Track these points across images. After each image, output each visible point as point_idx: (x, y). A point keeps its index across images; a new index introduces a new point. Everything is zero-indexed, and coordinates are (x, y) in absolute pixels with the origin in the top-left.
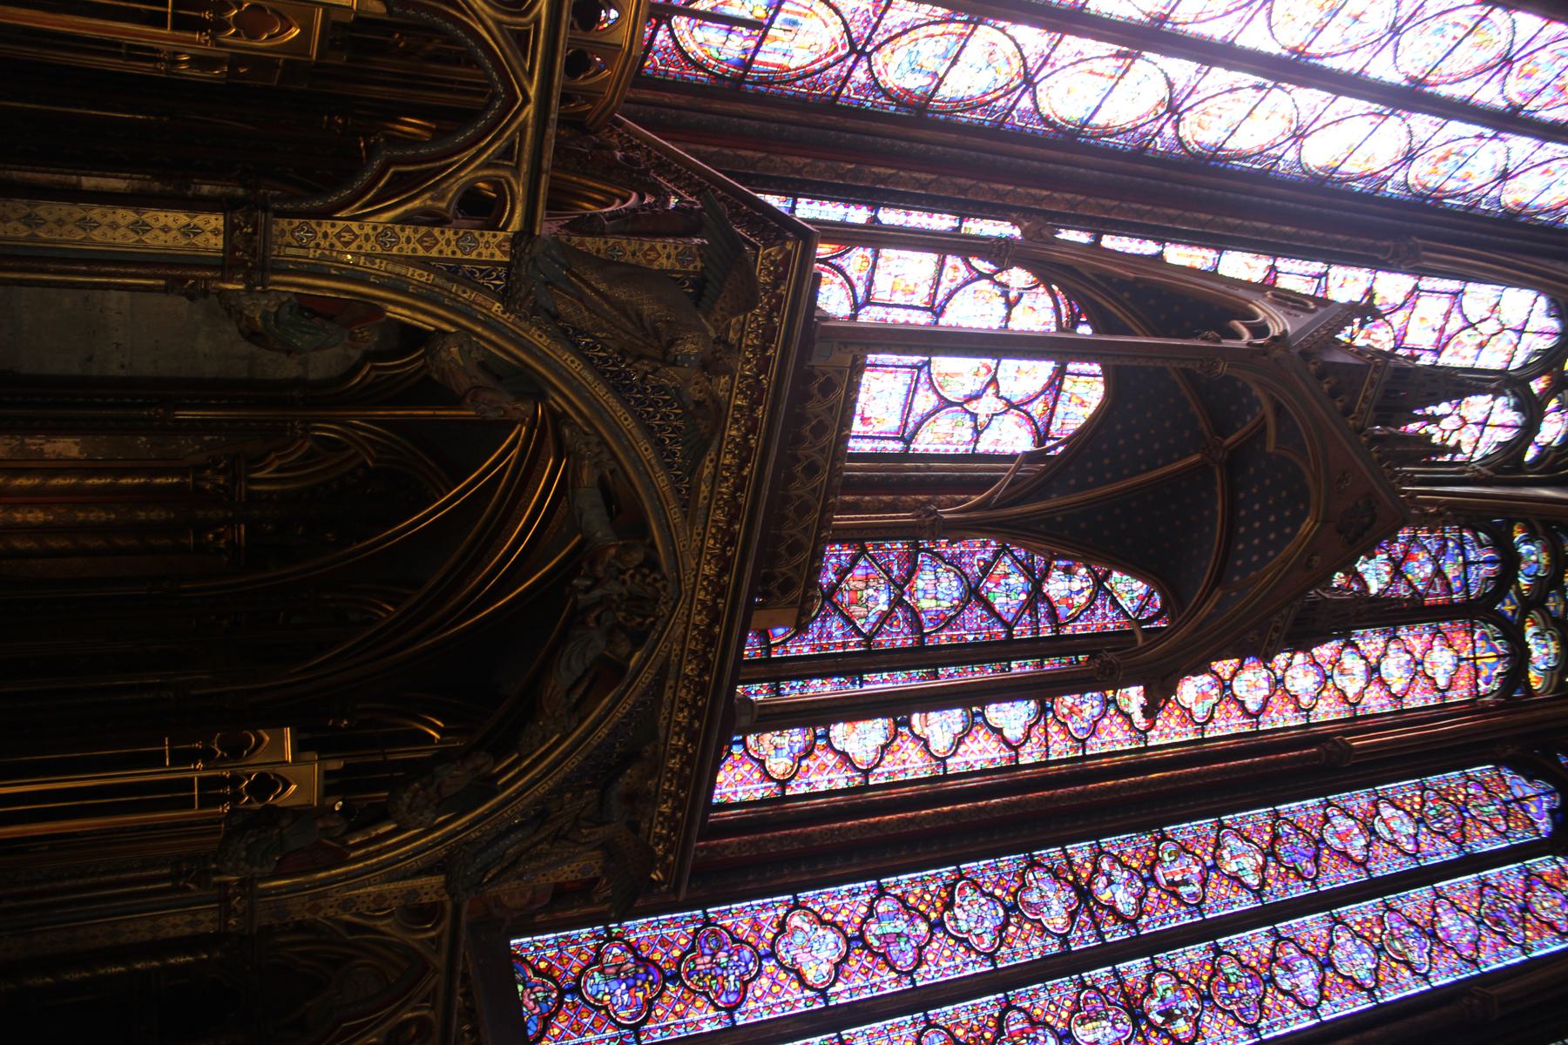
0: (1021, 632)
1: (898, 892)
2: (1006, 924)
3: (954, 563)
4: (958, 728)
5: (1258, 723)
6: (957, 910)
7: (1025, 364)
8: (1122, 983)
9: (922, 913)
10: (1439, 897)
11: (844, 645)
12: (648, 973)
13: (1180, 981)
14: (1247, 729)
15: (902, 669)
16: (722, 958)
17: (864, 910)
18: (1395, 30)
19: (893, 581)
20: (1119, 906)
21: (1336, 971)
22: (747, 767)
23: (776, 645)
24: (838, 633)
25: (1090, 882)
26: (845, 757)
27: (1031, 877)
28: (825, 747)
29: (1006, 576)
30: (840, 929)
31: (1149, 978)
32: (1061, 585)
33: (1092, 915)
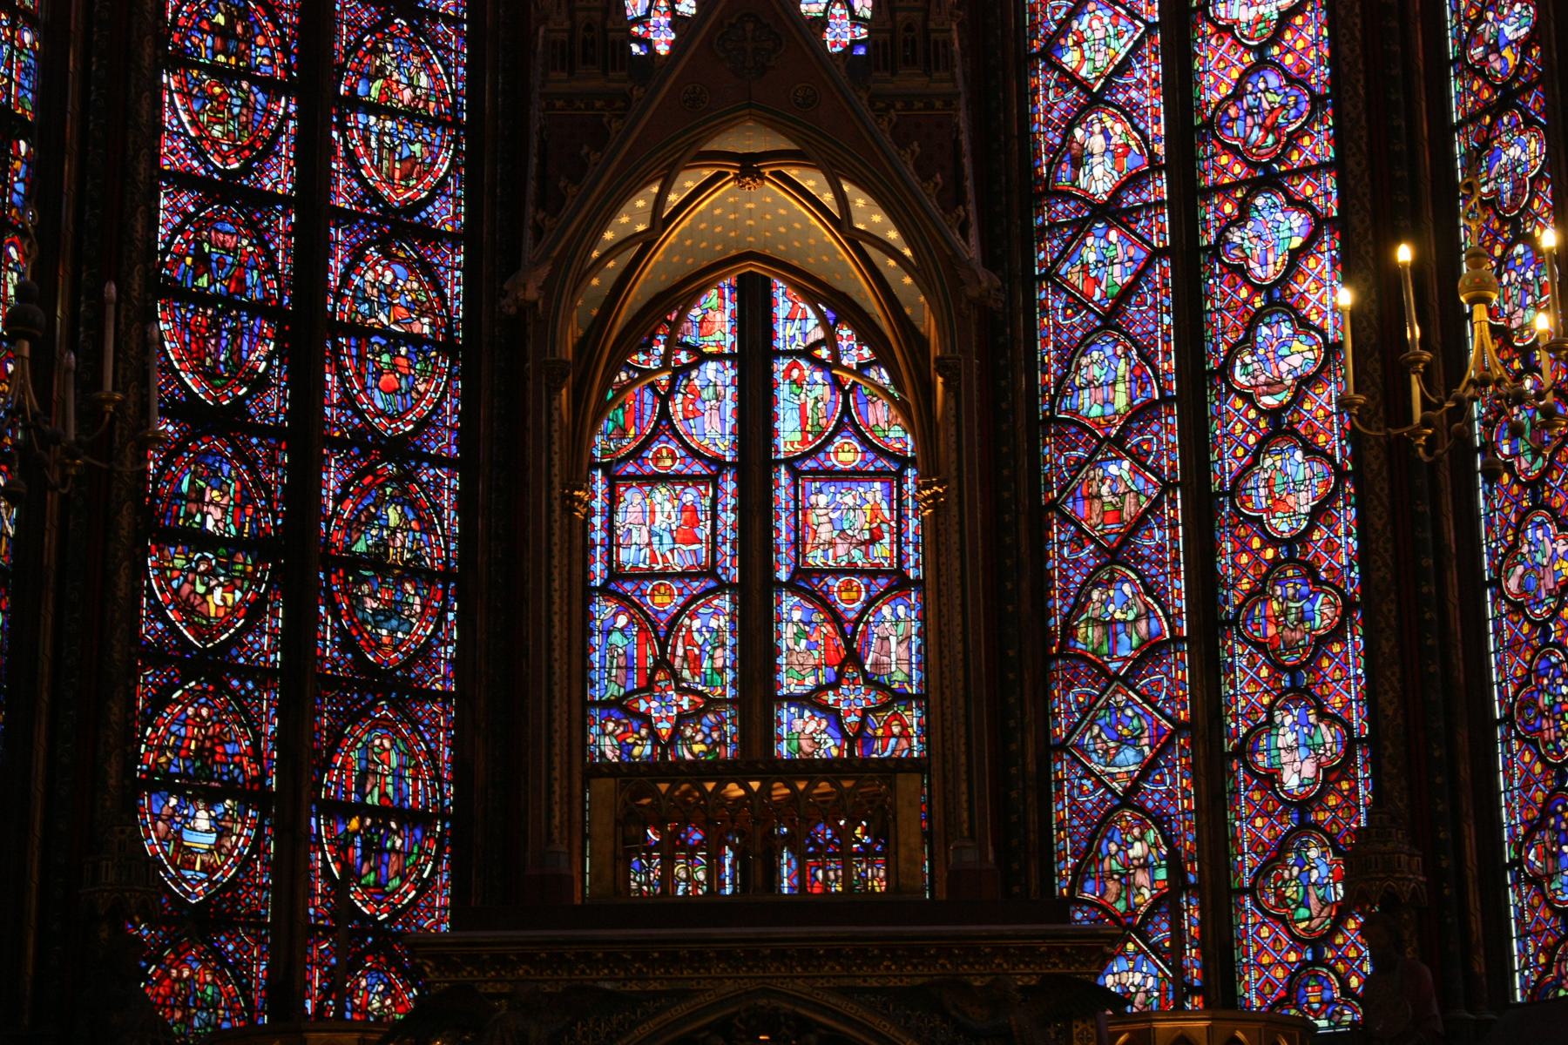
3: (1070, 356)
4: (1286, 329)
6: (1514, 325)
7: (782, 309)
11: (1173, 527)
12: (1555, 814)
15: (1206, 429)
16: (1546, 700)
19: (1093, 454)
22: (1325, 663)
23: (1172, 629)
26: (1319, 513)
27: (1485, 190)
28: (1304, 546)
29: (1085, 267)
30: (1523, 515)
32: (1098, 172)
33: (1528, 88)
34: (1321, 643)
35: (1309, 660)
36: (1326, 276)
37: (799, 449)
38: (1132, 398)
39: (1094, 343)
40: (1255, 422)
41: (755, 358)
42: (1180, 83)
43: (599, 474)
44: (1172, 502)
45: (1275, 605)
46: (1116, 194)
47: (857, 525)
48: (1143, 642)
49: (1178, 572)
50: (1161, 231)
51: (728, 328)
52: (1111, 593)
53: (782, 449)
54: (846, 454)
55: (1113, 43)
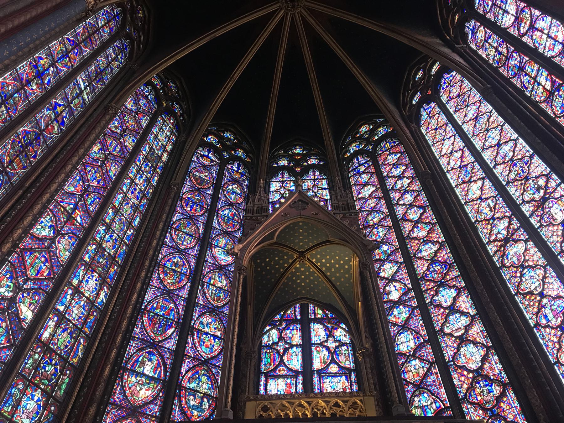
0: (414, 303)
1: (534, 317)
2: (530, 267)
4: (457, 315)
5: (427, 206)
7: (313, 334)
8: (534, 212)
9: (539, 304)
10: (464, 122)
11: (436, 374)
13: (524, 191)
14: (430, 209)
15: (440, 346)
17: (548, 330)
18: (180, 251)
20: (506, 225)
21: (500, 140)
22: (502, 404)
23: (444, 405)
24: (432, 377)
25: (501, 241)
26: (484, 359)
29: (395, 316)
31: (528, 202)
33: (513, 234)
34: (499, 399)
35: (496, 405)
36: (465, 300)
37: (321, 368)
38: (416, 343)
39: (401, 333)
40: (454, 341)
41: (307, 347)
42: (412, 272)
43: (263, 376)
44: (434, 368)
45: (478, 389)
46: (400, 298)
47: (339, 387)
48: (435, 410)
49: (441, 387)
50: (415, 303)
51: (299, 338)
52: (421, 397)
53: (315, 368)
54: (334, 369)
55: (393, 268)
